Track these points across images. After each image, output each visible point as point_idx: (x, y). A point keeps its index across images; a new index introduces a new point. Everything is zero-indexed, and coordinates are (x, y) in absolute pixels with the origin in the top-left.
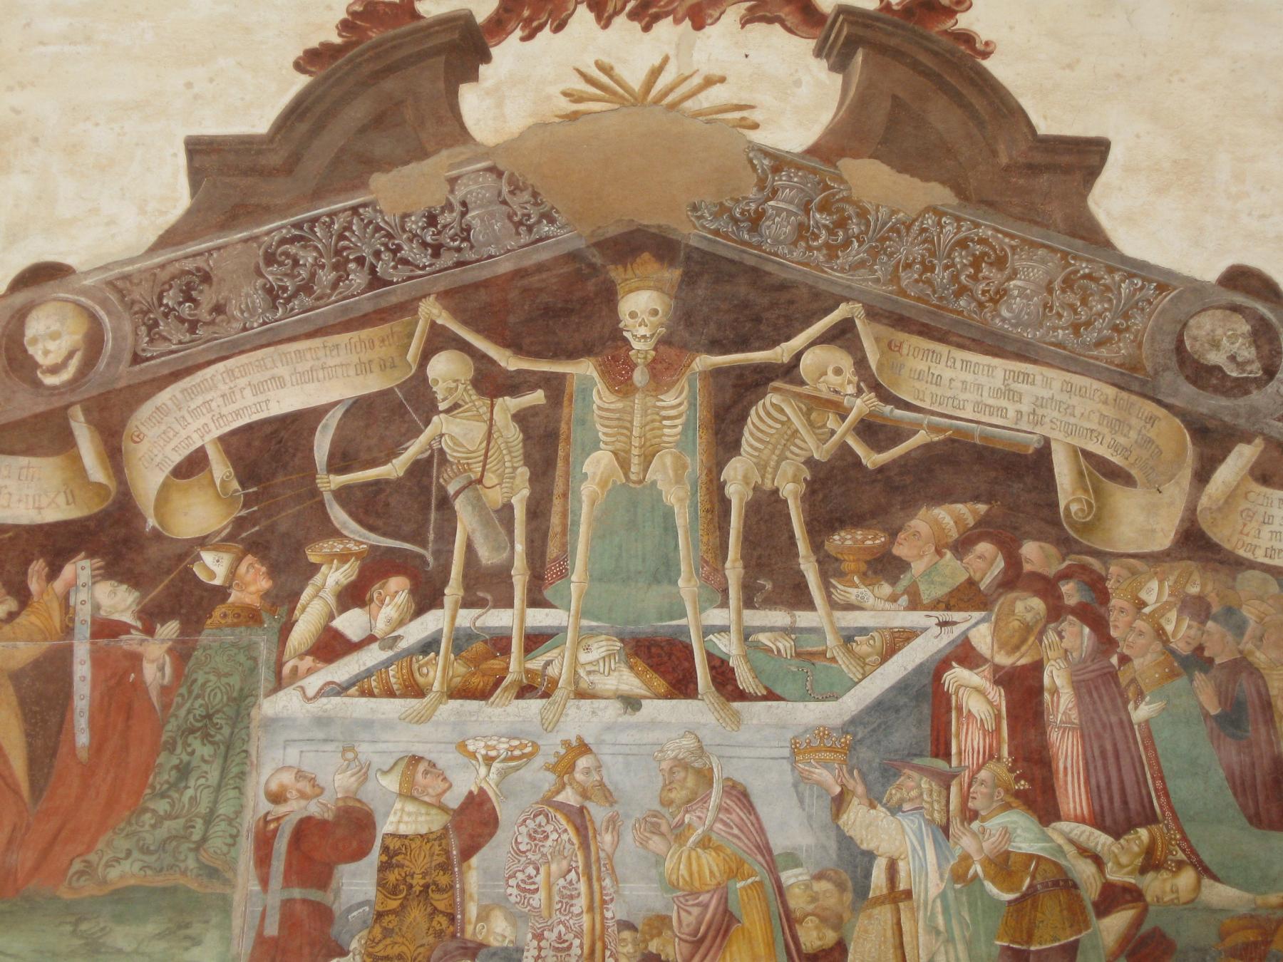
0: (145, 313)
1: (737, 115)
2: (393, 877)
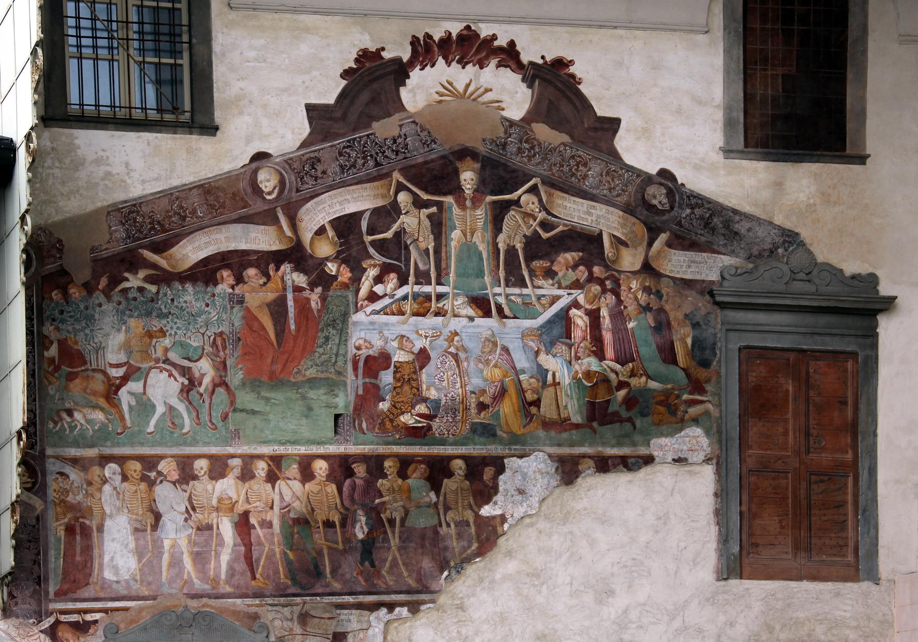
0: (299, 173)
1: (497, 104)
2: (398, 375)
